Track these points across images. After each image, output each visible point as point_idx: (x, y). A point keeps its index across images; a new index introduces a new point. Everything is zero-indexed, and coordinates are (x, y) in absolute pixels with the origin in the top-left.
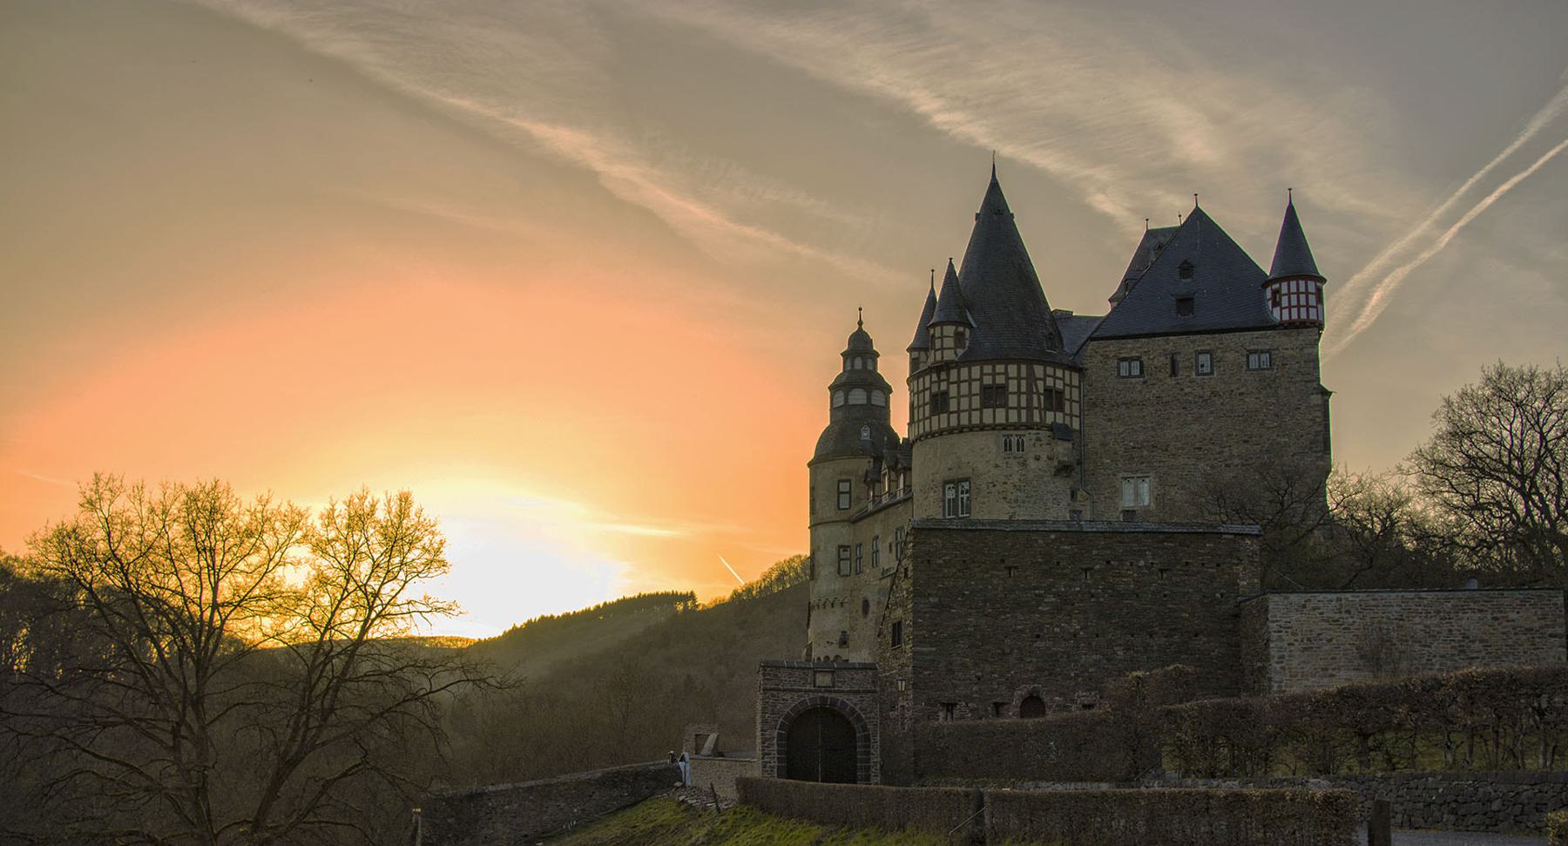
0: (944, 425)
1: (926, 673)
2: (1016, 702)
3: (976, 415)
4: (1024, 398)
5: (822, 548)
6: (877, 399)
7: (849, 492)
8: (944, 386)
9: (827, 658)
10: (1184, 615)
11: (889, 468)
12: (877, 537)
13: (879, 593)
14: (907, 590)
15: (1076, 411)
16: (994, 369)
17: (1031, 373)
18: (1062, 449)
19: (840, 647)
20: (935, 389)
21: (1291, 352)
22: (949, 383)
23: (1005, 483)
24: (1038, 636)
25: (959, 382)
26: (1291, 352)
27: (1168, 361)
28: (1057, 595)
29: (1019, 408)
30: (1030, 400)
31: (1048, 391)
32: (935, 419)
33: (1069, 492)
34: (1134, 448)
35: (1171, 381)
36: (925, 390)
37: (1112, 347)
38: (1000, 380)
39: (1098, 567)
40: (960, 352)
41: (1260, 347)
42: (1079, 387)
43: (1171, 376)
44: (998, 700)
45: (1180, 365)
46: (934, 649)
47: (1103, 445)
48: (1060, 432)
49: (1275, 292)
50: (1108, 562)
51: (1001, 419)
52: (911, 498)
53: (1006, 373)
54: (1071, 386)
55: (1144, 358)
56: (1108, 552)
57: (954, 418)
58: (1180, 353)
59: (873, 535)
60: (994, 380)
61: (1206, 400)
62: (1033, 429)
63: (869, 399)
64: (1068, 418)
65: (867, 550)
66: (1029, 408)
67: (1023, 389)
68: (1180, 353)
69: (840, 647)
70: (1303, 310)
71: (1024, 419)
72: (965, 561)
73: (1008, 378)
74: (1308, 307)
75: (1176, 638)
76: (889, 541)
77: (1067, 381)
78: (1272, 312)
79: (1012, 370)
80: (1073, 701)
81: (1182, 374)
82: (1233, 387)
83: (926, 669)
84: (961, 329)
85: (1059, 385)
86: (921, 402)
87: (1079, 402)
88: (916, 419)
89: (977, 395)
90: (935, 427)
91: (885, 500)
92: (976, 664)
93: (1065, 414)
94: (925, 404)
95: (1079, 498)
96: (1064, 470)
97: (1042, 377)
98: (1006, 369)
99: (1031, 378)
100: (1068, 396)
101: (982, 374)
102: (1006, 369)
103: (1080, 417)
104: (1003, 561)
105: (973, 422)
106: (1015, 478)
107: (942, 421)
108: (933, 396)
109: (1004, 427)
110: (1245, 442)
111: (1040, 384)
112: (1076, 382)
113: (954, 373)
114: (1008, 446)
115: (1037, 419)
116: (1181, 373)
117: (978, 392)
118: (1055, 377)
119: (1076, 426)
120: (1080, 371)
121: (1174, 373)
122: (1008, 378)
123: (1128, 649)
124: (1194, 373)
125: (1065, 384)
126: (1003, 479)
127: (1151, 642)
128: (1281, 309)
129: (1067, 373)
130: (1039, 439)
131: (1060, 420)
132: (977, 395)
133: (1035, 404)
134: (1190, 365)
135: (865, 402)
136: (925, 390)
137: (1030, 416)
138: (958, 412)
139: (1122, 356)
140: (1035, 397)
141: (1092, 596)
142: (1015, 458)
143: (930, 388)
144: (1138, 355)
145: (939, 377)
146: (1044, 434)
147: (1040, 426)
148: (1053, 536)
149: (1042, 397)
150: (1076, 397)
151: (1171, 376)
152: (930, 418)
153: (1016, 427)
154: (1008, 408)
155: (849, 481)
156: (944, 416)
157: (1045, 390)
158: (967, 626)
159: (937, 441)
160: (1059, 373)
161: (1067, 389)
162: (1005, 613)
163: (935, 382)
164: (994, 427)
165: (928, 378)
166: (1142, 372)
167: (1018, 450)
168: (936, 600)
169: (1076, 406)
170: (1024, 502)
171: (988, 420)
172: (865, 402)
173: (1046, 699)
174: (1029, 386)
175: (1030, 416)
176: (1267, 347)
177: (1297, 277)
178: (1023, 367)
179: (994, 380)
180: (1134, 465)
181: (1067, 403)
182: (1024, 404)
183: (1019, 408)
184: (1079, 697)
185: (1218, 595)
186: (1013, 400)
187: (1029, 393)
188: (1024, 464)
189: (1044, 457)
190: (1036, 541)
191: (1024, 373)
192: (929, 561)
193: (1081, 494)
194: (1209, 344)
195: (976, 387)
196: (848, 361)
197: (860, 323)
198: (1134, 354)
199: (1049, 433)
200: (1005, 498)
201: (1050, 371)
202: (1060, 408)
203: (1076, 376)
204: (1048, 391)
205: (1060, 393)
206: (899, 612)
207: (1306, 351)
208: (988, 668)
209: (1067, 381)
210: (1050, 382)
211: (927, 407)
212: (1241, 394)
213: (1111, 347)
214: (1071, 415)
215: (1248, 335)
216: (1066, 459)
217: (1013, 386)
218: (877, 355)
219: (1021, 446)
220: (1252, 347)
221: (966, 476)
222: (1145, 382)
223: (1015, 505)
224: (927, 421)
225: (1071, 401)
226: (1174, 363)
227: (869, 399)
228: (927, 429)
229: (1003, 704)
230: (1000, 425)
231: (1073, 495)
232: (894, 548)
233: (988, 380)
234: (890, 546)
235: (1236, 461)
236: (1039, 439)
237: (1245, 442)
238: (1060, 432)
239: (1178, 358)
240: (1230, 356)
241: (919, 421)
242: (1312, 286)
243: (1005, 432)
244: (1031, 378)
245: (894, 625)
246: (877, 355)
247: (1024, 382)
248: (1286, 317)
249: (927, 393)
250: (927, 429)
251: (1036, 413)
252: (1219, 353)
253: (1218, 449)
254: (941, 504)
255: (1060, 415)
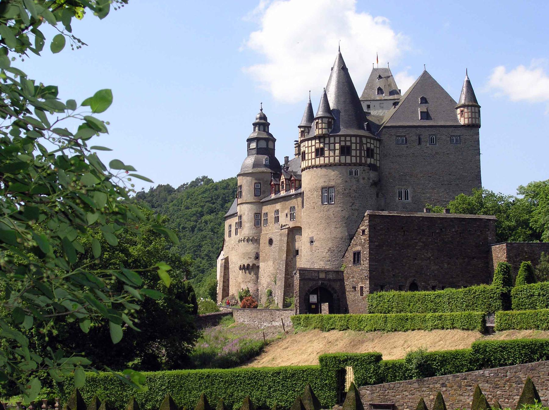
0: (322, 162)
1: (374, 273)
2: (408, 285)
3: (337, 158)
4: (358, 152)
5: (246, 214)
6: (270, 146)
7: (260, 189)
8: (322, 145)
9: (248, 265)
10: (469, 251)
11: (286, 179)
12: (278, 210)
13: (281, 235)
14: (365, 239)
15: (378, 158)
16: (345, 139)
17: (361, 141)
18: (373, 175)
19: (255, 260)
20: (317, 146)
21: (468, 137)
22: (325, 144)
23: (350, 189)
24: (416, 259)
25: (329, 144)
26: (468, 137)
27: (417, 138)
28: (423, 242)
29: (356, 156)
30: (361, 153)
31: (368, 149)
32: (317, 159)
33: (376, 194)
34: (402, 175)
35: (418, 147)
36: (312, 146)
37: (393, 131)
38: (348, 144)
39: (437, 231)
40: (330, 130)
41: (455, 134)
42: (379, 148)
43: (418, 145)
44: (401, 284)
45: (423, 140)
46: (377, 263)
47: (389, 173)
48: (373, 167)
49: (462, 111)
50: (441, 229)
51: (348, 161)
52: (301, 195)
53: (351, 141)
54: (376, 147)
55: (407, 136)
56: (441, 225)
57: (327, 159)
58: (422, 135)
59: (275, 209)
60: (345, 144)
61: (433, 156)
62: (361, 165)
63: (267, 145)
64: (375, 161)
65: (271, 216)
66: (361, 157)
67: (358, 148)
68: (422, 135)
69: (255, 260)
70: (474, 119)
71: (358, 161)
72: (388, 228)
73: (351, 143)
74: (475, 118)
75: (466, 260)
76: (286, 211)
77: (375, 145)
78: (460, 119)
79: (353, 140)
80: (429, 284)
81: (423, 144)
82: (445, 151)
83: (374, 272)
84: (330, 120)
85: (372, 146)
86: (310, 151)
87: (379, 154)
88: (306, 158)
89: (338, 150)
90: (317, 163)
91: (283, 193)
92: (393, 270)
93: (374, 160)
94: (312, 152)
95: (380, 197)
96: (375, 184)
97: (365, 143)
98: (351, 139)
99: (361, 143)
100: (375, 152)
101: (340, 141)
102: (351, 139)
103: (379, 161)
104: (402, 228)
105: (336, 162)
106: (354, 187)
107: (320, 161)
108: (317, 150)
109: (350, 164)
110: (450, 174)
111: (365, 146)
112: (378, 146)
113: (327, 141)
114: (351, 173)
115: (363, 161)
116: (423, 143)
117: (338, 148)
118: (371, 143)
119: (378, 165)
120: (380, 140)
121: (420, 143)
122: (351, 143)
123: (449, 264)
124: (428, 144)
125: (374, 147)
126: (350, 188)
127: (457, 261)
128: (465, 118)
129: (375, 141)
130: (364, 170)
131: (372, 162)
132: (338, 150)
133: (363, 155)
134: (426, 140)
135: (265, 146)
136: (312, 146)
137: (361, 159)
138: (329, 157)
139: (397, 135)
140: (363, 151)
141: (436, 243)
142: (354, 178)
143: (315, 145)
144: (404, 135)
145: (320, 141)
146: (366, 168)
147: (364, 165)
148: (421, 219)
149: (366, 152)
150: (378, 152)
151: (418, 145)
152: (315, 159)
153: (355, 164)
154: (351, 156)
155: (260, 183)
156: (322, 158)
157: (367, 149)
158: (389, 254)
159: (319, 169)
160: (372, 142)
161: (375, 148)
162: (403, 249)
163: (317, 143)
164: (345, 164)
165: (313, 142)
166: (406, 142)
167: (355, 175)
168: (378, 244)
169: (378, 156)
170: (358, 198)
171: (343, 161)
172: (265, 146)
173: (419, 284)
174: (360, 147)
175: (361, 159)
176: (459, 134)
177: (471, 106)
178: (358, 138)
179: (345, 144)
180: (402, 183)
181: (375, 155)
182: (358, 155)
183: (356, 156)
184: (431, 283)
185: (481, 243)
186: (353, 153)
187: (360, 150)
188: (358, 181)
189: (366, 178)
190: (415, 221)
191: (358, 141)
192: (375, 228)
193: (380, 194)
194: (434, 132)
195: (337, 146)
196: (257, 128)
197: (261, 110)
198: (403, 134)
199: (368, 168)
200: (350, 196)
201: (369, 141)
202: (372, 157)
203: (378, 143)
204: (368, 149)
205: (372, 150)
206: (359, 248)
207: (474, 137)
208: (397, 271)
209: (375, 145)
210: (369, 145)
211: (314, 154)
212: (448, 154)
213: (393, 131)
214: (377, 160)
215: (451, 129)
216: (376, 179)
217: (354, 147)
218: (269, 124)
219: (356, 173)
220: (452, 134)
221: (332, 185)
222: (407, 147)
223: (354, 199)
224: (313, 160)
225: (376, 153)
226: (419, 139)
227: (267, 145)
228: (313, 163)
229: (402, 286)
230: (348, 163)
231: (377, 195)
232: (289, 215)
233: (343, 144)
234: (287, 215)
235: (446, 183)
236: (364, 170)
237: (450, 174)
238: (373, 167)
239: (421, 137)
240: (444, 137)
241: (308, 160)
242: (477, 109)
243: (350, 167)
244: (361, 143)
245: (354, 254)
246: (269, 124)
247: (358, 145)
248: (466, 122)
249: (313, 148)
250: (313, 163)
251: (363, 158)
252: (438, 136)
253: (438, 177)
254: (320, 197)
255: (372, 160)
